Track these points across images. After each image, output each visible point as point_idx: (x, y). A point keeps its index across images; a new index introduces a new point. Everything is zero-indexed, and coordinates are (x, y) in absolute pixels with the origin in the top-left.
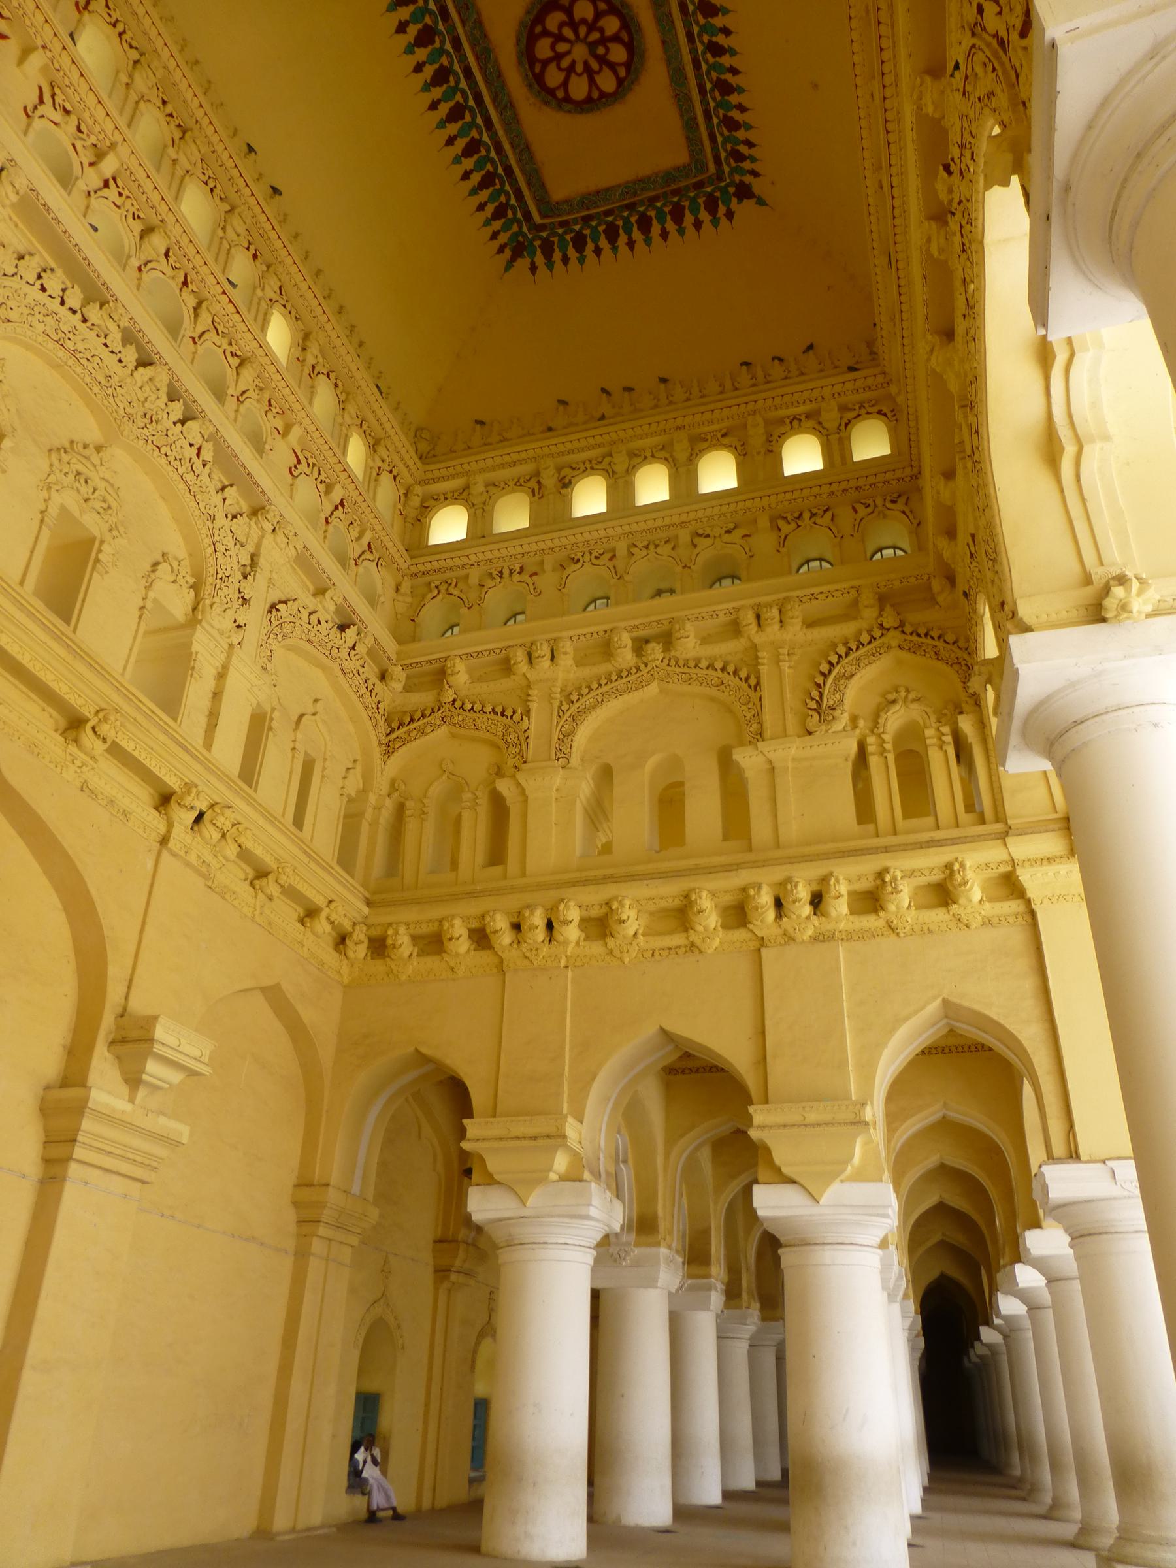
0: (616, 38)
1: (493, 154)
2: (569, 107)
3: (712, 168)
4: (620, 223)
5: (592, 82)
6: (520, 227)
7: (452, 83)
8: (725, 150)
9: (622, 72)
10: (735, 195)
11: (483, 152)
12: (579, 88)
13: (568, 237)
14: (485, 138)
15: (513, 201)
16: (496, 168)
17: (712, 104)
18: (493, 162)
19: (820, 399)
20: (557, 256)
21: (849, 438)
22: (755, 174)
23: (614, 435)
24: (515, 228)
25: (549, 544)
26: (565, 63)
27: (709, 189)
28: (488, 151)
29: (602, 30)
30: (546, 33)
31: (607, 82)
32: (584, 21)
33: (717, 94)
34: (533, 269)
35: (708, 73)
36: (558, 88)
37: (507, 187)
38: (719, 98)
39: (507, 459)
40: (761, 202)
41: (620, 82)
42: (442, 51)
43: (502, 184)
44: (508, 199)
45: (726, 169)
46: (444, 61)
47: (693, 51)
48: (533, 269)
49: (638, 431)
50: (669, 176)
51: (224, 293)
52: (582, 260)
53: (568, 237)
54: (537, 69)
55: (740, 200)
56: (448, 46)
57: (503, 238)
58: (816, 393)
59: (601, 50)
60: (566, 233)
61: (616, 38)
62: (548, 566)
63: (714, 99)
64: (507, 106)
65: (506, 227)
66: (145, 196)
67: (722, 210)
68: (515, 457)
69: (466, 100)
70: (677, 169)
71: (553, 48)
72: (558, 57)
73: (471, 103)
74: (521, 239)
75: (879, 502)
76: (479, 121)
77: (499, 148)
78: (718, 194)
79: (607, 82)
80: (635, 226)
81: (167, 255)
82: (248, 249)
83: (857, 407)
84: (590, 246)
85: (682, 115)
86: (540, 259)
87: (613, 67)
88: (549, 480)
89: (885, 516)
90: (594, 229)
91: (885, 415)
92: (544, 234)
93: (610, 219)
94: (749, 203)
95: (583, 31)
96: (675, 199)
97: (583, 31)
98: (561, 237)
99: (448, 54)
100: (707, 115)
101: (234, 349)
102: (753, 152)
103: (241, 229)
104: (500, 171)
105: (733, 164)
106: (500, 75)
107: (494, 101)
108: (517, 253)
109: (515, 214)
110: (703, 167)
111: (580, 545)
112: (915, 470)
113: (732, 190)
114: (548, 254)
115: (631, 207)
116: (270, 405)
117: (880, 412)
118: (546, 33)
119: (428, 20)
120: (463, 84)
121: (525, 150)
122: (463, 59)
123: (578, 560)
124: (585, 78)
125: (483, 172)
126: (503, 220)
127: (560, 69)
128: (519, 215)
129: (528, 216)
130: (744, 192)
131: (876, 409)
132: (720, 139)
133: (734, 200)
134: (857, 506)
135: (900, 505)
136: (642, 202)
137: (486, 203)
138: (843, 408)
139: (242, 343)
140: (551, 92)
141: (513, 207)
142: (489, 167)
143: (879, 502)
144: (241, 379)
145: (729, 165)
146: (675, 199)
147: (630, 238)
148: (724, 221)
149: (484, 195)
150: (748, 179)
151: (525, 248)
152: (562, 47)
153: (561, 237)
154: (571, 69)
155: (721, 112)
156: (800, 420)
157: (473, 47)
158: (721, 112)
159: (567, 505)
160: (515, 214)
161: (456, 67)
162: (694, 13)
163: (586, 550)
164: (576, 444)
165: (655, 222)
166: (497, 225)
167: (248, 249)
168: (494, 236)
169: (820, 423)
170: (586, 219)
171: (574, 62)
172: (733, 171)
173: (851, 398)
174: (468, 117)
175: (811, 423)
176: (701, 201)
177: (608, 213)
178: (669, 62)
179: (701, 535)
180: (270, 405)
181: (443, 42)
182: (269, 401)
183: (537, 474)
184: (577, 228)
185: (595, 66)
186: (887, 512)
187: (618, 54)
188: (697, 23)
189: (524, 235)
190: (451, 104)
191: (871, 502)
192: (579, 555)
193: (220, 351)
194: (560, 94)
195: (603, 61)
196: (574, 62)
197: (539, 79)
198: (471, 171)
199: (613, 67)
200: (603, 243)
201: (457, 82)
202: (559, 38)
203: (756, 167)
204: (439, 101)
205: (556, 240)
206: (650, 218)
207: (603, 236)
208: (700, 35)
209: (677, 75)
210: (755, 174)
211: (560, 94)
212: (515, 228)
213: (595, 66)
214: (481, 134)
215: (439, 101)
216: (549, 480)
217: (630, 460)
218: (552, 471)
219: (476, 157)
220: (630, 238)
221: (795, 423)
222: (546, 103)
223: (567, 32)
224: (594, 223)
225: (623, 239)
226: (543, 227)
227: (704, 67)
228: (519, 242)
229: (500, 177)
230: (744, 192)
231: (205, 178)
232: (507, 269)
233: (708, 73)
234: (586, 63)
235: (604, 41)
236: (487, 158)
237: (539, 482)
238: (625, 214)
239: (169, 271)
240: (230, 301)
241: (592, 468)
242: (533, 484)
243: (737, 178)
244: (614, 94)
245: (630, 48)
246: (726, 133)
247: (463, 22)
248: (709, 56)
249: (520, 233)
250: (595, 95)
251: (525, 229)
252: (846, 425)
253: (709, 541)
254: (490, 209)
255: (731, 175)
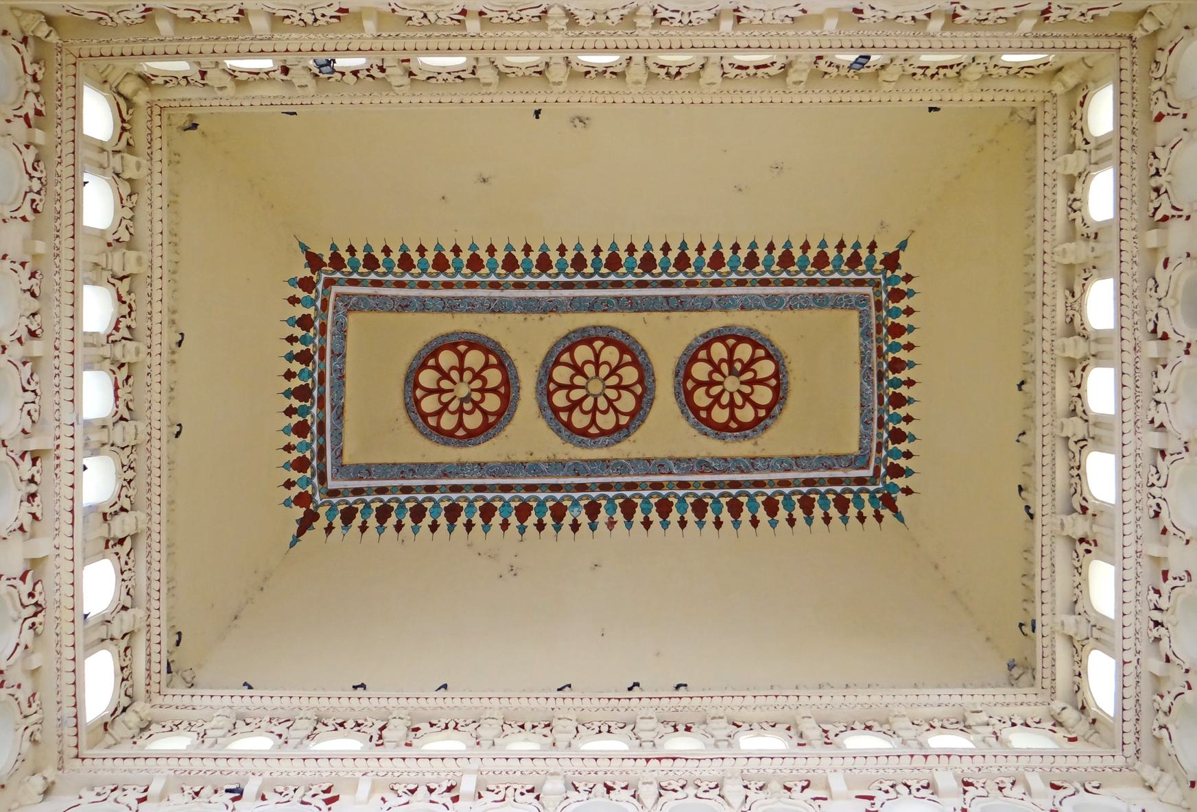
0: (731, 351)
1: (787, 490)
2: (776, 409)
3: (868, 290)
4: (891, 390)
5: (762, 382)
6: (868, 491)
7: (710, 501)
8: (849, 272)
9: (761, 353)
10: (893, 272)
11: (780, 498)
12: (763, 395)
13: (891, 447)
14: (769, 491)
15: (838, 489)
16: (800, 493)
17: (802, 276)
18: (793, 493)
19: (1055, 176)
20: (903, 462)
21: (1097, 138)
22: (872, 247)
23: (1046, 431)
24: (865, 496)
25: (1129, 540)
26: (739, 400)
27: (884, 296)
28: (781, 494)
29: (722, 360)
30: (709, 409)
31: (765, 368)
32: (710, 374)
33: (792, 269)
34: (908, 491)
35: (773, 273)
36: (756, 413)
37: (823, 489)
38: (796, 268)
39: (1046, 573)
40: (903, 245)
41: (768, 356)
42: (682, 500)
43: (817, 492)
44: (835, 493)
45: (868, 275)
46: (690, 500)
47: (754, 283)
48: (908, 491)
49: (1047, 399)
50: (866, 334)
51: (648, 760)
52: (913, 438)
53: (891, 447)
54: (733, 425)
55: (897, 266)
56: (681, 493)
57: (868, 511)
58: (1049, 181)
59: (738, 366)
60: (887, 448)
61: (731, 351)
62: (1155, 550)
63: (797, 273)
64: (752, 463)
65: (859, 504)
66: (518, 773)
67: (902, 286)
68: (1047, 563)
69: (730, 495)
70: (861, 324)
71: (723, 407)
72: (732, 405)
73: (734, 492)
74: (878, 495)
75: (1156, 85)
76: (752, 491)
77: (785, 483)
78: (889, 288)
79: (765, 368)
80: (897, 375)
81: (576, 789)
82: (676, 730)
83: (1073, 132)
84: (902, 426)
85: (810, 308)
86: (901, 482)
87: (753, 360)
88: (1080, 526)
89: (1174, 76)
90: (893, 418)
91: (1085, 97)
92: (883, 470)
93: (886, 400)
94: (903, 258)
95: (717, 377)
96: (884, 330)
97: (717, 377)
98: (890, 454)
99: (687, 495)
100: (812, 283)
101: (704, 787)
102: (849, 243)
103: (652, 724)
104: (805, 490)
105: (863, 267)
106: (725, 460)
107: (742, 472)
108: (889, 503)
109: (851, 492)
110: (863, 299)
111: (1139, 497)
112: (1126, 42)
113: (889, 274)
114: (896, 471)
115: (881, 376)
116: (789, 789)
117: (1082, 104)
118: (709, 409)
119: (653, 501)
120: (716, 493)
121: (797, 462)
122: (697, 485)
123: (1158, 505)
124: (756, 387)
125: (797, 505)
126: (851, 505)
127: (741, 407)
128: (855, 488)
129: (860, 481)
130: (891, 261)
131: (1078, 108)
132: (836, 276)
133: (898, 272)
134: (1155, 114)
135: (1162, 57)
136: (879, 365)
137: (826, 514)
138: (1072, 148)
139: (705, 774)
140: (758, 420)
141: (844, 491)
142: (795, 498)
143: (1156, 85)
144: (727, 796)
145: (864, 272)
146: (884, 330)
147: (905, 383)
148: (911, 285)
149: (818, 512)
150: (879, 255)
151: (889, 494)
152: (725, 399)
153: (890, 454)
154: (746, 398)
155: (809, 268)
156: (1075, 200)
157: (692, 472)
158: (809, 268)
159: (1103, 509)
160: (851, 492)
161: (700, 493)
162: (720, 274)
163: (1146, 490)
164: (1047, 480)
165: (897, 355)
166: (852, 511)
167: (676, 730)
168: (861, 518)
169: (1080, 174)
170: (881, 424)
171: (739, 391)
172: (870, 268)
173: (1061, 140)
174: (744, 499)
175: (1078, 187)
176: (891, 305)
177: (881, 402)
178: (759, 307)
179: (1156, 325)
180: (789, 789)
181: (676, 496)
182: (786, 788)
183: (1070, 539)
184: (885, 435)
185: (748, 376)
186: (1168, 74)
187: (744, 352)
188: (729, 273)
189: (878, 491)
190: (725, 508)
191: (1154, 98)
192: (1153, 502)
193: (692, 799)
194: (762, 413)
195: (747, 367)
196: (739, 391)
197: (743, 427)
198: (790, 515)
199: (753, 360)
200: (902, 411)
201: (712, 497)
202: (717, 399)
203: (865, 244)
204: (717, 518)
205: (890, 460)
206: (894, 358)
207: (898, 411)
208: (738, 273)
209: (773, 303)
210: (872, 247)
211: (762, 413)
212: (865, 496)
213: (748, 376)
214: (763, 494)
215: (717, 518)
216: (1080, 526)
217: (1076, 415)
218: (1068, 520)
219: (781, 506)
220: (905, 383)
221: (1076, 205)
222: (766, 428)
223: (715, 390)
224: (886, 417)
225: (903, 390)
226: (877, 469)
227: (767, 276)
228: (881, 498)
229: (809, 492)
230: (891, 261)
231: (597, 730)
232: (902, 520)
233: (773, 273)
234: (742, 383)
235: (730, 361)
236: (788, 498)
237: (1082, 540)
238: (885, 383)
239: (584, 795)
240: (660, 759)
241: (1079, 468)
242: (1081, 548)
243: (878, 266)
244: (777, 364)
245: (741, 339)
246: (830, 268)
247: (670, 473)
248: (758, 269)
249: (872, 495)
250: (773, 382)
251: (872, 488)
252: (1087, 143)
253: (1163, 314)
254: (833, 512)
255: (874, 272)
